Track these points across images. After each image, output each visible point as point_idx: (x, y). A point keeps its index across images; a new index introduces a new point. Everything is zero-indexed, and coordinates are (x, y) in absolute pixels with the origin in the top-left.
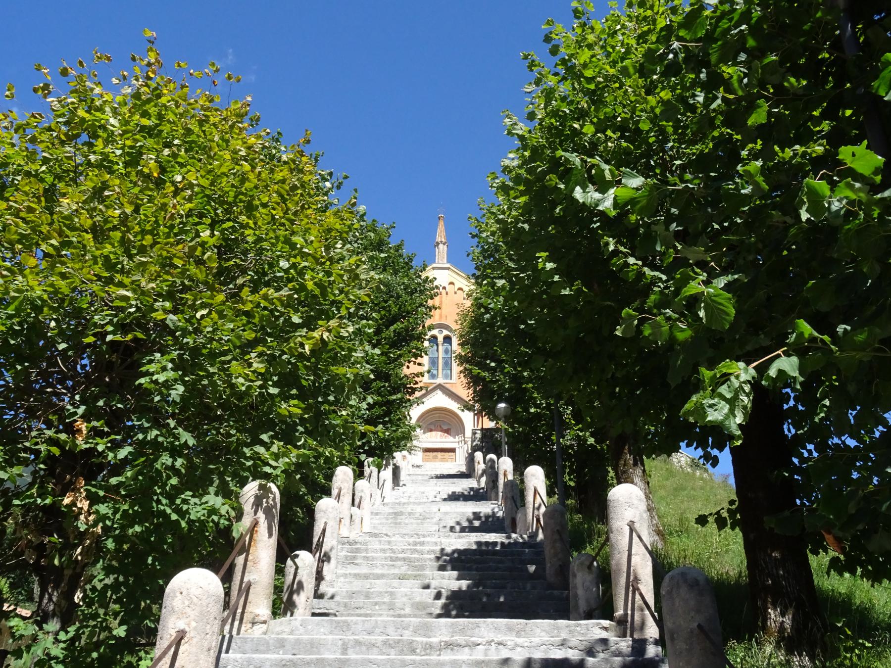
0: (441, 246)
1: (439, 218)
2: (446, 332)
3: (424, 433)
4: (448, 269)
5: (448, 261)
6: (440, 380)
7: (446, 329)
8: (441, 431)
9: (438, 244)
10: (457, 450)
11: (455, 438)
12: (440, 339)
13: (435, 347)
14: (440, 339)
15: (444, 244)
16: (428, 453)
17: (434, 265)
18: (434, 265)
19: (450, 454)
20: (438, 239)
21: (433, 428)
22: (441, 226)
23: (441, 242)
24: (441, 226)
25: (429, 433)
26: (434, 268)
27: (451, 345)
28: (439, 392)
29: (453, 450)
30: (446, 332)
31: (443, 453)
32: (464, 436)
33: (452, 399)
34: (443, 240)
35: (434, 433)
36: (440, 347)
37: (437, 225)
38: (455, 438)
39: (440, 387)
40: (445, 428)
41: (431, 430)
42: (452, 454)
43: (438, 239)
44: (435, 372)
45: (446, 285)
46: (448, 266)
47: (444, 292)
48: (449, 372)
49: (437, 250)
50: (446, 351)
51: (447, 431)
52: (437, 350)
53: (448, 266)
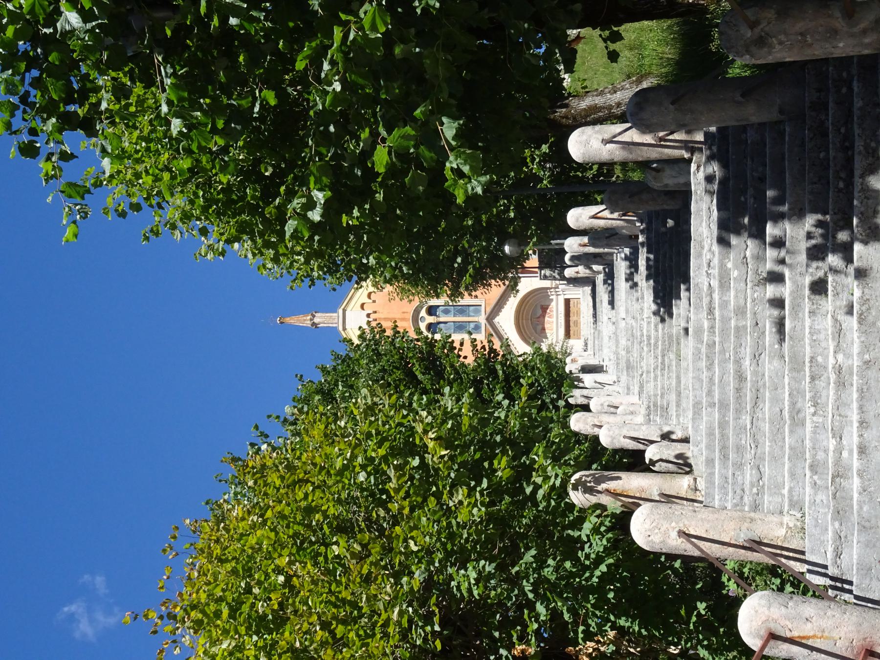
0: (316, 320)
1: (282, 323)
2: (423, 313)
3: (547, 338)
4: (344, 311)
5: (335, 311)
6: (482, 319)
8: (544, 317)
9: (314, 324)
12: (431, 319)
13: (442, 326)
14: (431, 319)
15: (314, 316)
16: (571, 332)
17: (341, 328)
18: (341, 328)
19: (571, 305)
20: (308, 323)
21: (540, 327)
22: (292, 320)
23: (311, 320)
24: (292, 320)
25: (547, 331)
26: (344, 329)
27: (438, 306)
28: (496, 320)
29: (567, 302)
30: (423, 313)
31: (571, 315)
32: (551, 288)
33: (505, 304)
34: (309, 318)
35: (546, 326)
36: (442, 319)
37: (291, 325)
39: (490, 319)
40: (540, 312)
41: (544, 329)
42: (571, 303)
43: (308, 323)
44: (472, 325)
45: (365, 313)
46: (340, 311)
47: (373, 316)
48: (472, 308)
49: (321, 325)
50: (446, 312)
51: (545, 309)
52: (445, 323)
53: (340, 311)
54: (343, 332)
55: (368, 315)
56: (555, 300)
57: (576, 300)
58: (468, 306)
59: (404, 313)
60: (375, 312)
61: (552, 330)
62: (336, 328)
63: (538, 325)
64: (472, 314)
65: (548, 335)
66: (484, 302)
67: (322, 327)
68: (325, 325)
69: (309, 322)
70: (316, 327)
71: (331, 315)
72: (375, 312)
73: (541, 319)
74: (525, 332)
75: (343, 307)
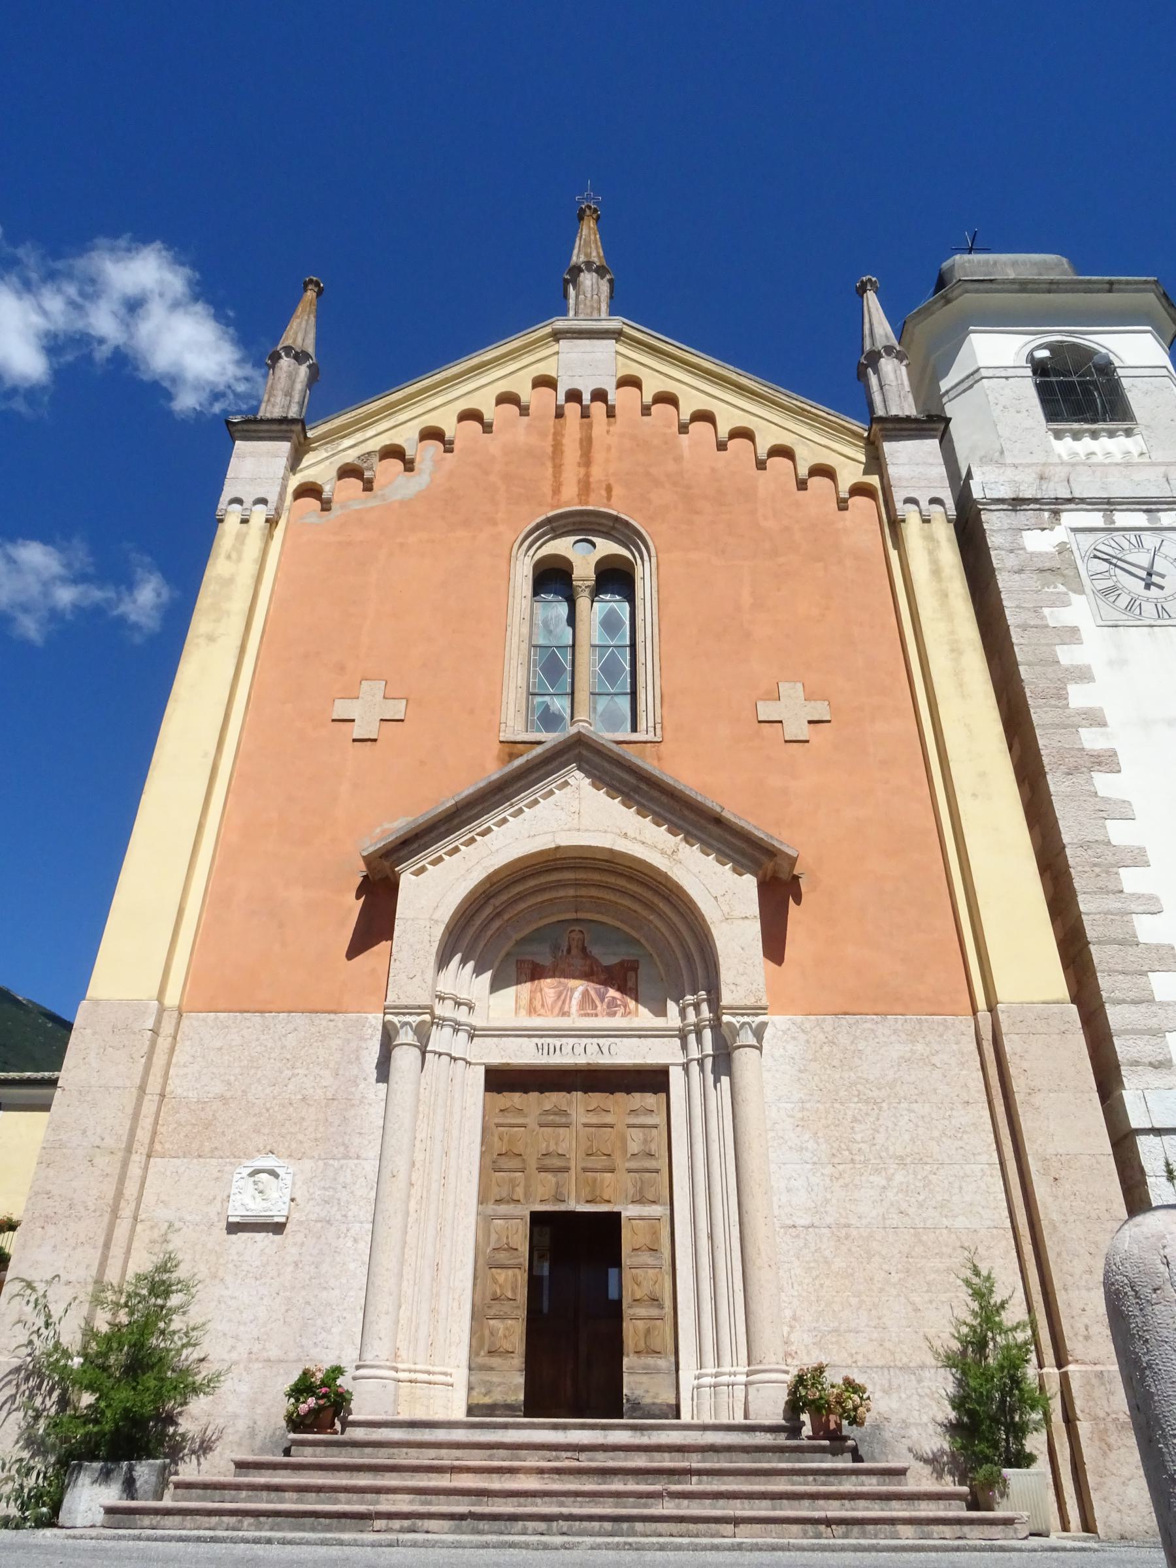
0: (588, 279)
1: (582, 211)
2: (606, 547)
3: (496, 985)
4: (617, 335)
5: (613, 312)
7: (607, 535)
8: (588, 976)
9: (576, 271)
10: (676, 1078)
11: (661, 1012)
13: (563, 609)
15: (601, 271)
16: (516, 1098)
17: (560, 324)
18: (560, 324)
21: (546, 960)
22: (588, 231)
23: (589, 264)
24: (588, 231)
25: (526, 987)
26: (557, 336)
27: (631, 599)
28: (578, 779)
30: (606, 547)
31: (596, 1099)
32: (714, 1002)
35: (549, 987)
36: (583, 602)
38: (661, 1012)
40: (609, 960)
41: (535, 973)
42: (650, 1100)
43: (577, 258)
44: (560, 705)
45: (609, 386)
46: (616, 323)
47: (598, 409)
48: (624, 703)
49: (572, 291)
50: (610, 624)
52: (572, 620)
53: (616, 323)
54: (548, 330)
55: (600, 395)
56: (659, 1022)
57: (659, 1120)
58: (634, 694)
59: (609, 489)
60: (611, 413)
61: (532, 1010)
62: (564, 312)
63: (556, 948)
64: (602, 703)
65: (509, 993)
66: (650, 737)
67: (566, 296)
68: (572, 302)
69: (582, 258)
70: (567, 282)
71: (604, 307)
72: (611, 413)
73: (578, 963)
74: (521, 897)
75: (627, 330)
